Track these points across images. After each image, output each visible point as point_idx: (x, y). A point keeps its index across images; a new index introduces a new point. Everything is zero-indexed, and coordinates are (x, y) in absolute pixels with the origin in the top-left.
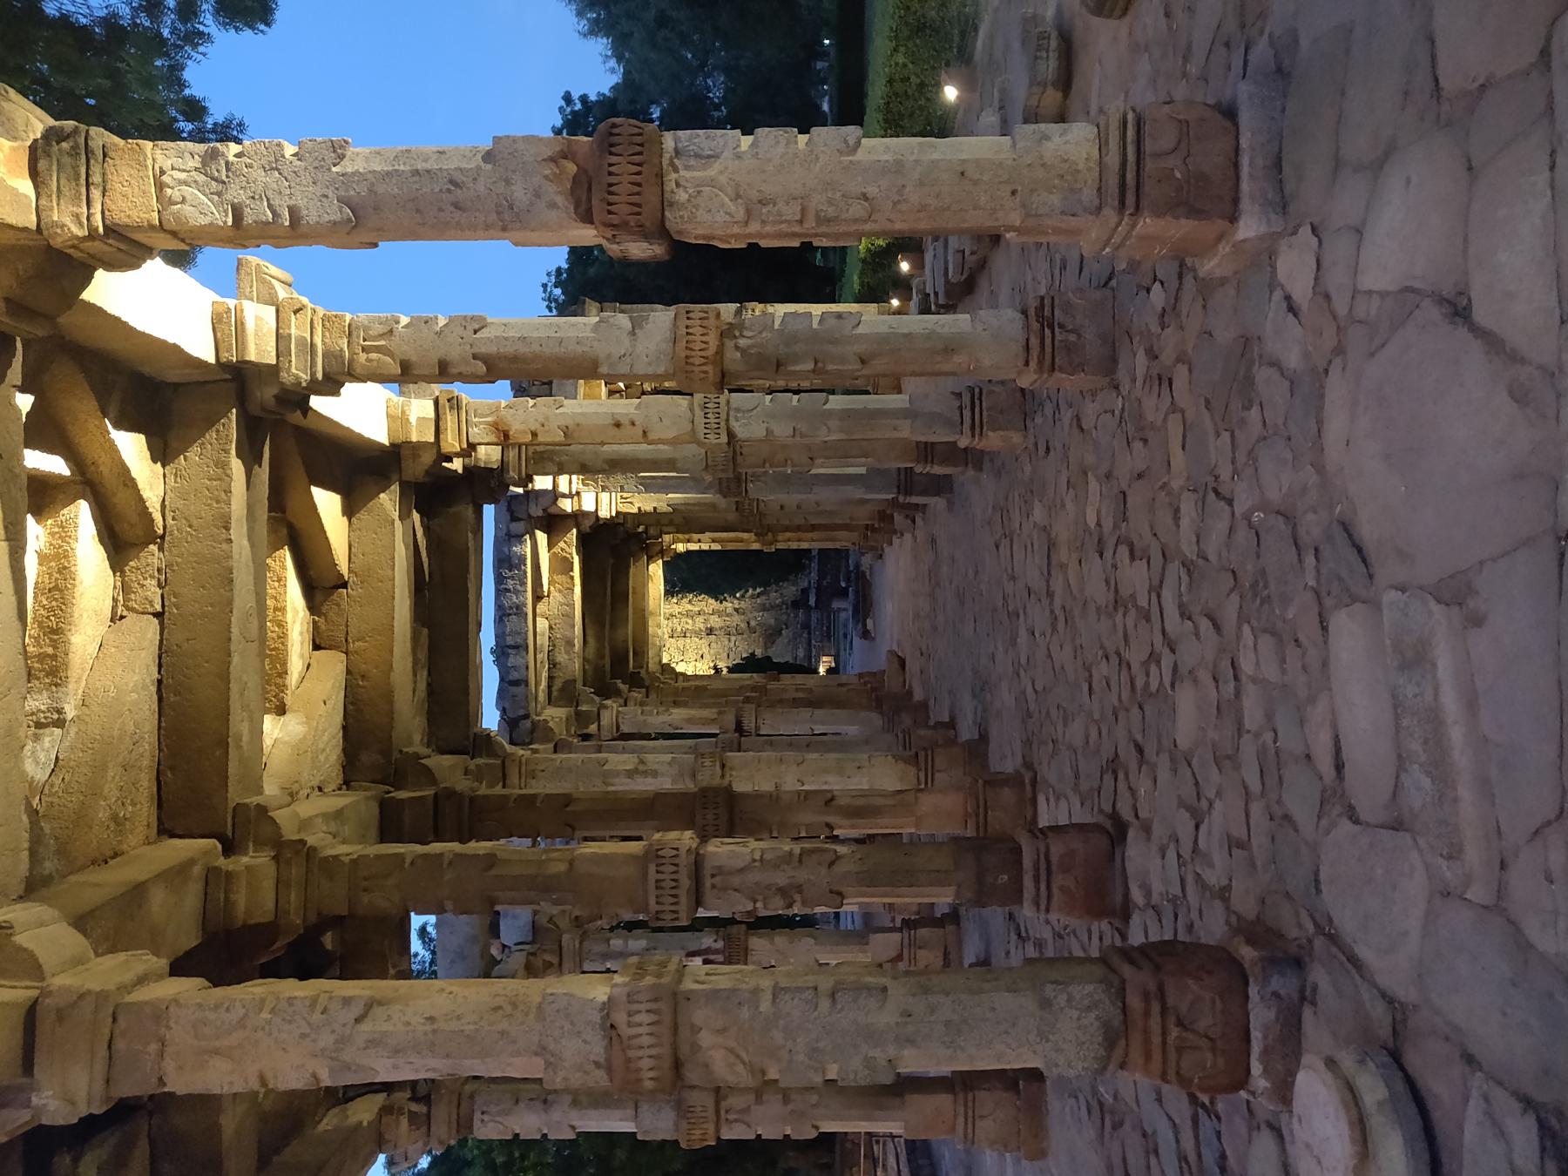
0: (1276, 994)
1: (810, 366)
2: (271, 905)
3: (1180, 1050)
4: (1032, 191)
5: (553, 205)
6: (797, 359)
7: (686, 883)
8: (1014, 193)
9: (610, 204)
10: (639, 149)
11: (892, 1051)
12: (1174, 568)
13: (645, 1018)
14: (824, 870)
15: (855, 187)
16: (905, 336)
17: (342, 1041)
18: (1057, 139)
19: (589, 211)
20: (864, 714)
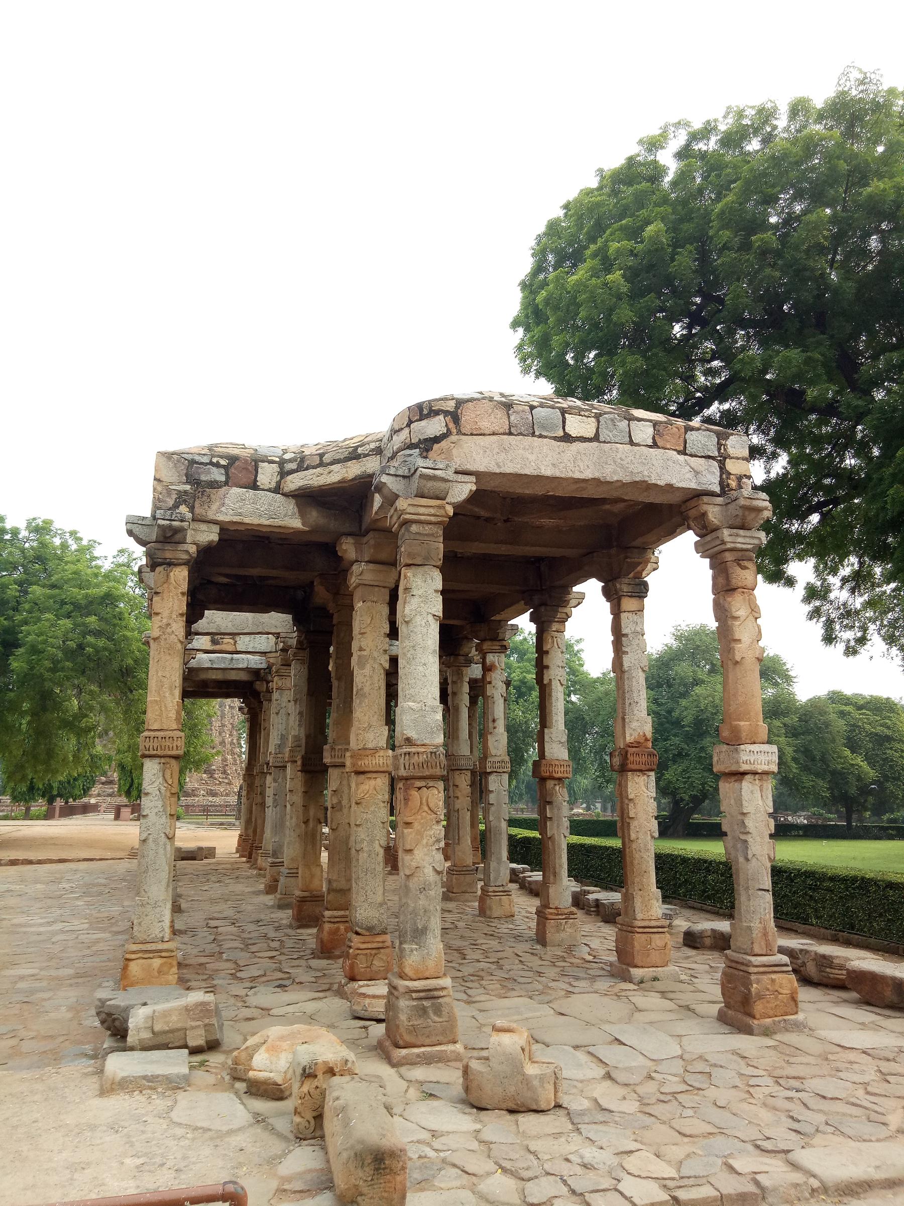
5: (631, 735)
11: (366, 849)
13: (381, 763)
15: (641, 835)
17: (375, 659)
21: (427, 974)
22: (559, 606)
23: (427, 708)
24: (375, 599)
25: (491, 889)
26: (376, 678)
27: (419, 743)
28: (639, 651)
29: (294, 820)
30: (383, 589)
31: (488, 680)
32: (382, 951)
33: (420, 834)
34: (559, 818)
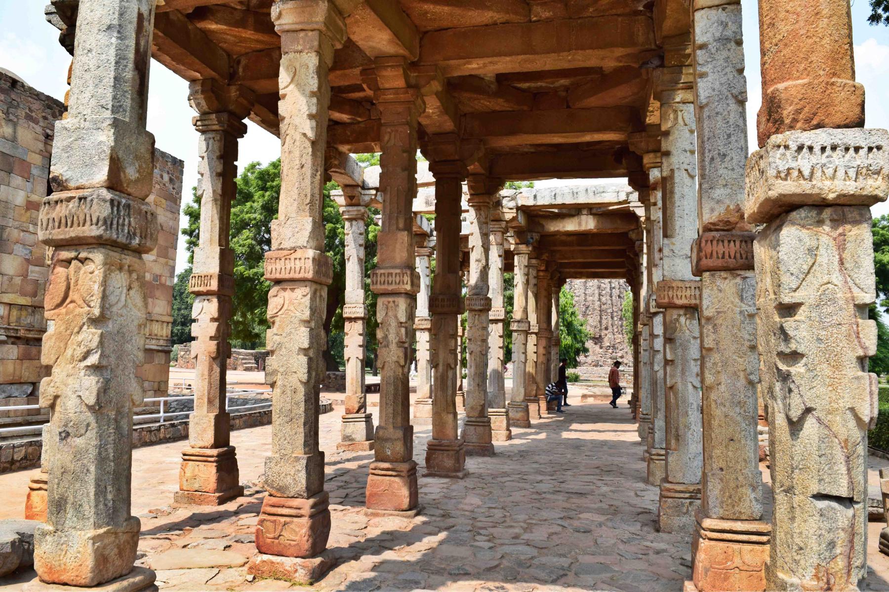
0: (296, 571)
1: (669, 357)
2: (387, 86)
3: (275, 521)
4: (721, 480)
5: (712, 210)
6: (673, 350)
7: (390, 288)
8: (722, 469)
9: (712, 241)
10: (744, 256)
11: (279, 383)
12: (535, 552)
14: (395, 359)
15: (723, 378)
16: (687, 412)
18: (753, 496)
19: (710, 230)
20: (522, 390)
21: (64, 578)
22: (681, 66)
23: (87, 124)
24: (300, 48)
25: (654, 451)
26: (297, 153)
27: (72, 184)
28: (728, 70)
29: (473, 369)
30: (310, 33)
31: (652, 200)
32: (295, 520)
33: (64, 339)
34: (685, 361)
